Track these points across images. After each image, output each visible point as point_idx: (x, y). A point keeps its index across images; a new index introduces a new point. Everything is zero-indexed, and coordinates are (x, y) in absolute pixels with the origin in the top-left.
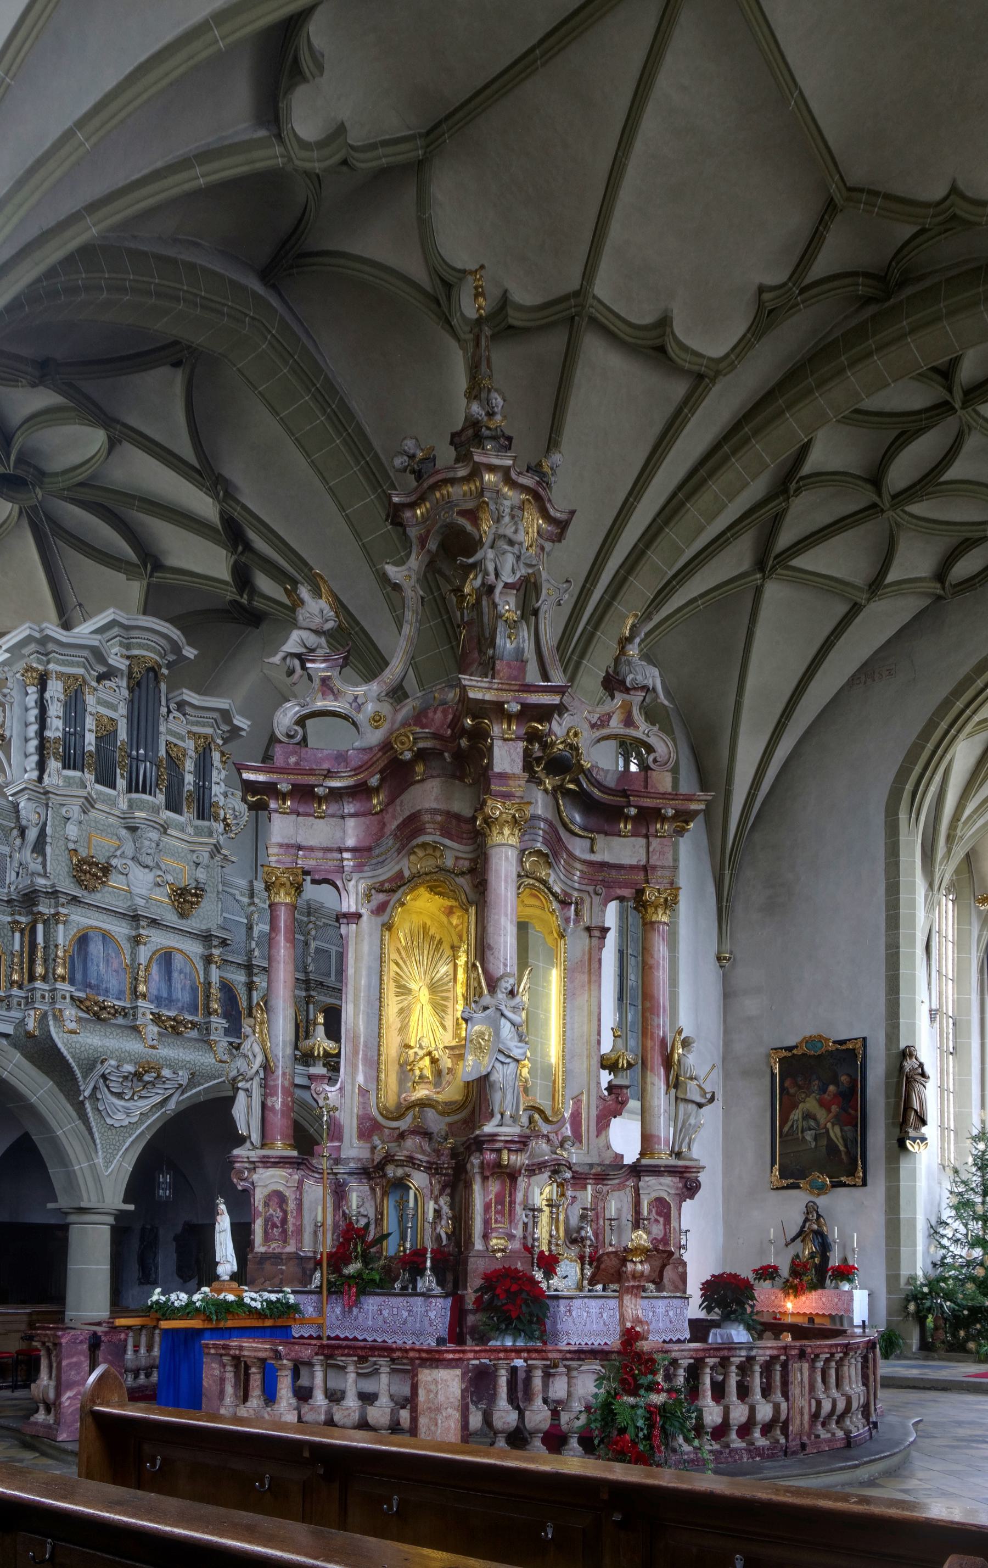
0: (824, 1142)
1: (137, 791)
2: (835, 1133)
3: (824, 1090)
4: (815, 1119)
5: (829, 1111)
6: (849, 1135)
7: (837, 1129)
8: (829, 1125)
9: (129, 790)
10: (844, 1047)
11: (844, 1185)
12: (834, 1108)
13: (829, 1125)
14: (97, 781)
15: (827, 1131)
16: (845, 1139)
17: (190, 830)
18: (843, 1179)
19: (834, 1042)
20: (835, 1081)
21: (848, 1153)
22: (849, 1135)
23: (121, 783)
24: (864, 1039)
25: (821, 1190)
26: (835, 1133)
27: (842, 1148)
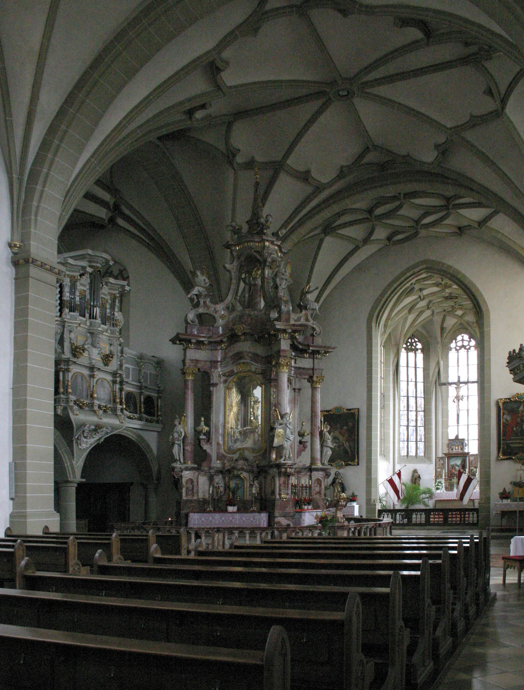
0: (342, 448)
1: (93, 318)
2: (346, 445)
3: (342, 428)
4: (339, 440)
5: (344, 436)
6: (352, 446)
7: (347, 443)
8: (344, 442)
9: (90, 318)
10: (350, 412)
11: (350, 465)
12: (346, 436)
13: (344, 442)
14: (80, 315)
15: (343, 444)
16: (350, 447)
17: (109, 331)
18: (349, 463)
19: (347, 410)
20: (347, 425)
21: (352, 452)
22: (352, 446)
23: (87, 315)
24: (358, 409)
25: (341, 467)
26: (346, 445)
27: (349, 450)
